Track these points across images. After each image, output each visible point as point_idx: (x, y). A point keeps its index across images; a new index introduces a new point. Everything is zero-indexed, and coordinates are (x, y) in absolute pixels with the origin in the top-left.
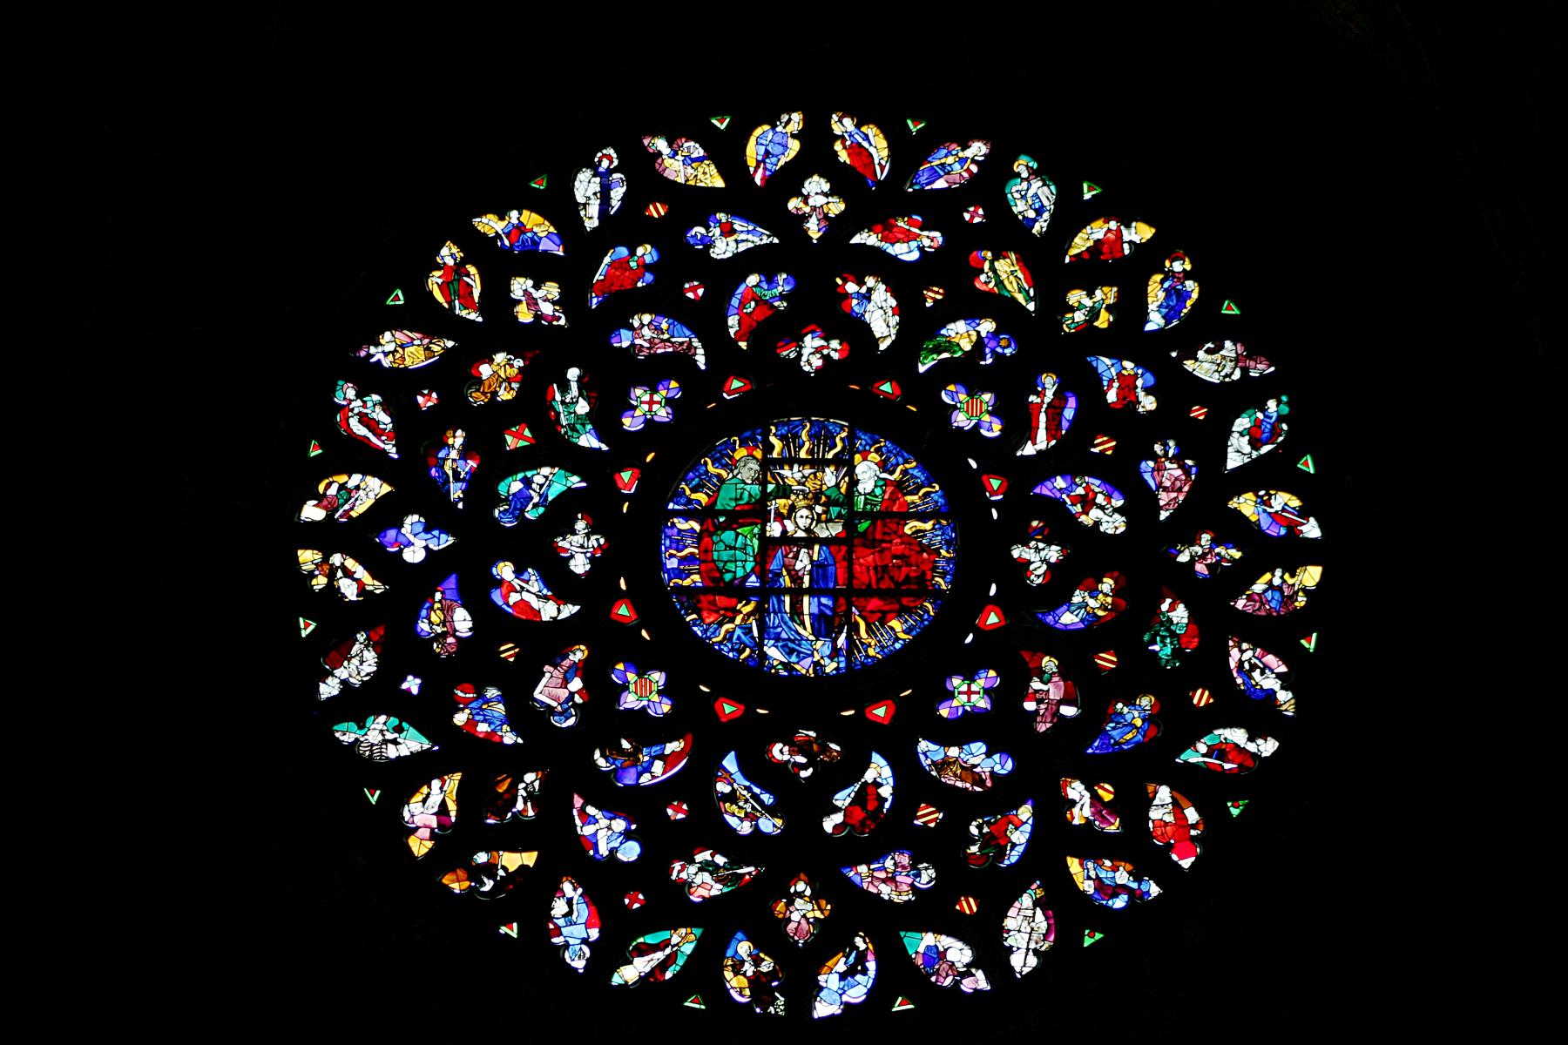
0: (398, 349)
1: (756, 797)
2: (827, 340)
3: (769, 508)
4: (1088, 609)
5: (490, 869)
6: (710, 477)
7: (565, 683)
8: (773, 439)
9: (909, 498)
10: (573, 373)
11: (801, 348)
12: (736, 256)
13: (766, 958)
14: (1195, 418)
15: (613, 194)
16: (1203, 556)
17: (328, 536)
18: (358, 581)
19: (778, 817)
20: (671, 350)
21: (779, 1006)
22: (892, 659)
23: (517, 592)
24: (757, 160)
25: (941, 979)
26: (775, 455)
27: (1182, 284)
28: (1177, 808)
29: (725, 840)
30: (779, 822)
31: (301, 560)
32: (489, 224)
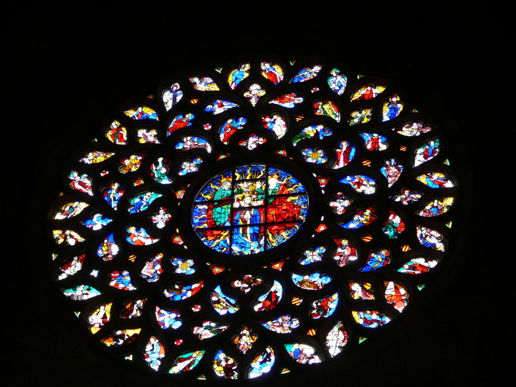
1: (227, 301)
3: (234, 198)
6: (212, 189)
7: (154, 266)
8: (236, 174)
9: (289, 189)
10: (160, 160)
11: (248, 142)
13: (230, 359)
16: (406, 199)
18: (76, 239)
19: (236, 307)
21: (235, 376)
22: (281, 246)
23: (136, 237)
24: (232, 81)
25: (301, 361)
27: (396, 105)
28: (397, 289)
31: (54, 234)
32: (131, 113)
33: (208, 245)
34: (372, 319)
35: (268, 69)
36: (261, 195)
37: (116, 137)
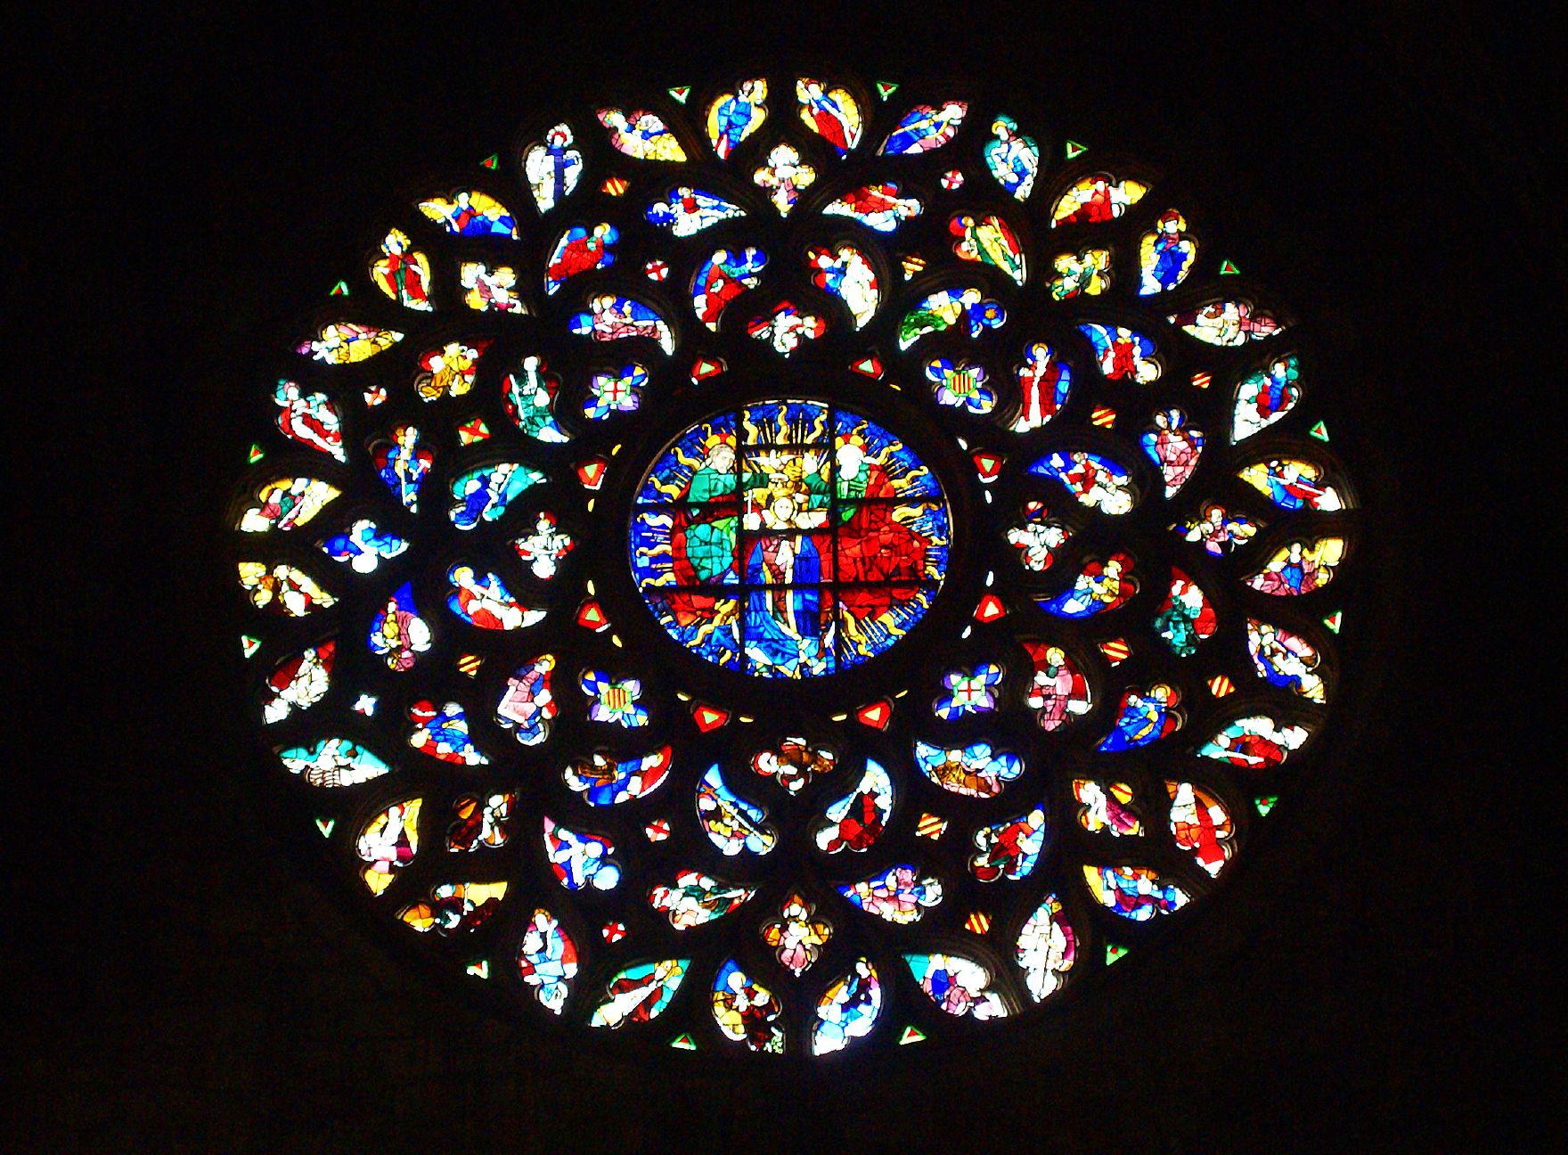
0: (343, 344)
1: (742, 813)
2: (801, 318)
4: (1094, 595)
5: (455, 904)
6: (681, 468)
7: (532, 695)
8: (747, 425)
9: (896, 483)
10: (531, 364)
11: (773, 327)
12: (702, 234)
14: (1198, 387)
15: (567, 171)
16: (1215, 534)
17: (272, 548)
18: (306, 595)
19: (768, 834)
20: (635, 334)
21: (776, 1043)
22: (885, 657)
25: (952, 1006)
26: (751, 441)
27: (1177, 245)
28: (1201, 808)
29: (710, 861)
30: (768, 840)
31: (242, 574)
32: (437, 210)
33: (680, 640)
34: (1140, 895)
35: (818, 102)
36: (818, 493)
37: (399, 281)
